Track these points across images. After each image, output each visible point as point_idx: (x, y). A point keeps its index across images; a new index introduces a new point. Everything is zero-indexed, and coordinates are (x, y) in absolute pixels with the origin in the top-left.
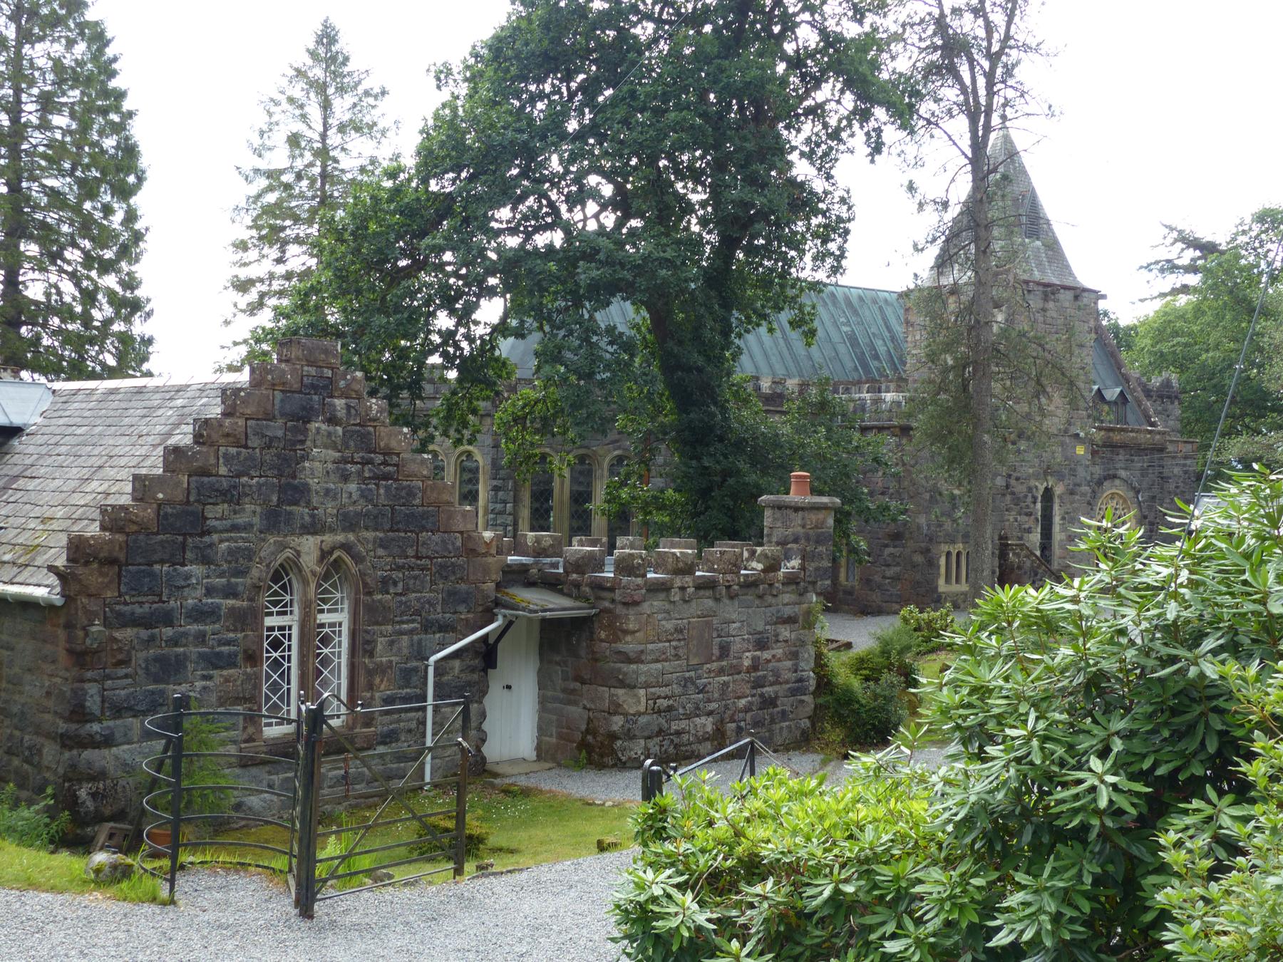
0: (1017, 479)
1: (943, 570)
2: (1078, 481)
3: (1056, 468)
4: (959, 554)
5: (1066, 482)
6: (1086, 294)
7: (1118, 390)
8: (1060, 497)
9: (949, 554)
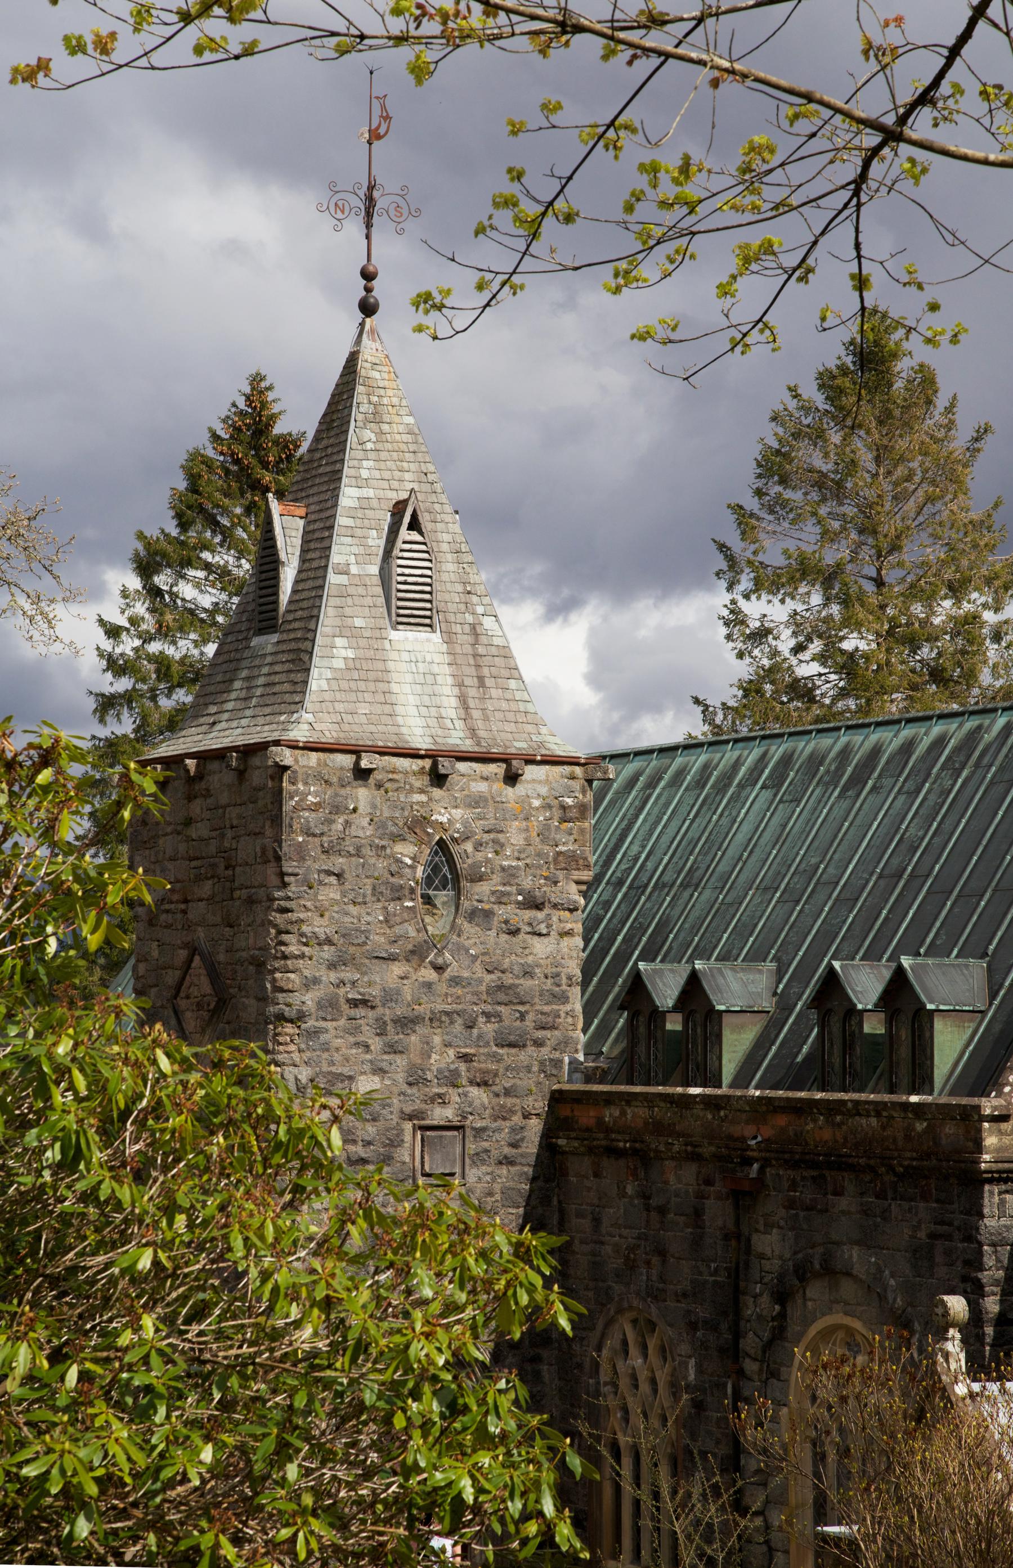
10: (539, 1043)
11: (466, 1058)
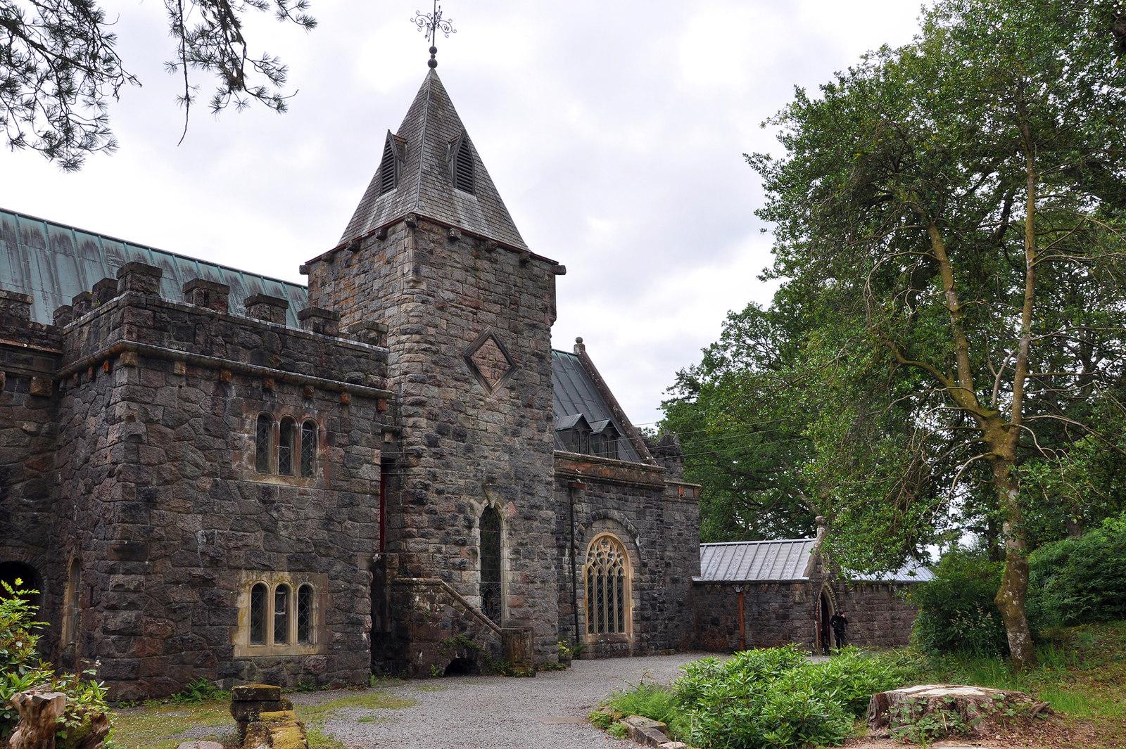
0: (440, 492)
1: (245, 619)
2: (536, 501)
3: (502, 481)
4: (282, 588)
5: (519, 502)
6: (537, 263)
7: (606, 422)
9: (259, 591)
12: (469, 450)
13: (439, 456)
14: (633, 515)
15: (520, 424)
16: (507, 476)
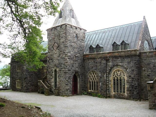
2: (62, 68)
8: (58, 72)
10: (82, 51)
11: (78, 51)
12: (53, 61)
13: (49, 63)
14: (126, 63)
15: (60, 55)
16: (58, 64)
